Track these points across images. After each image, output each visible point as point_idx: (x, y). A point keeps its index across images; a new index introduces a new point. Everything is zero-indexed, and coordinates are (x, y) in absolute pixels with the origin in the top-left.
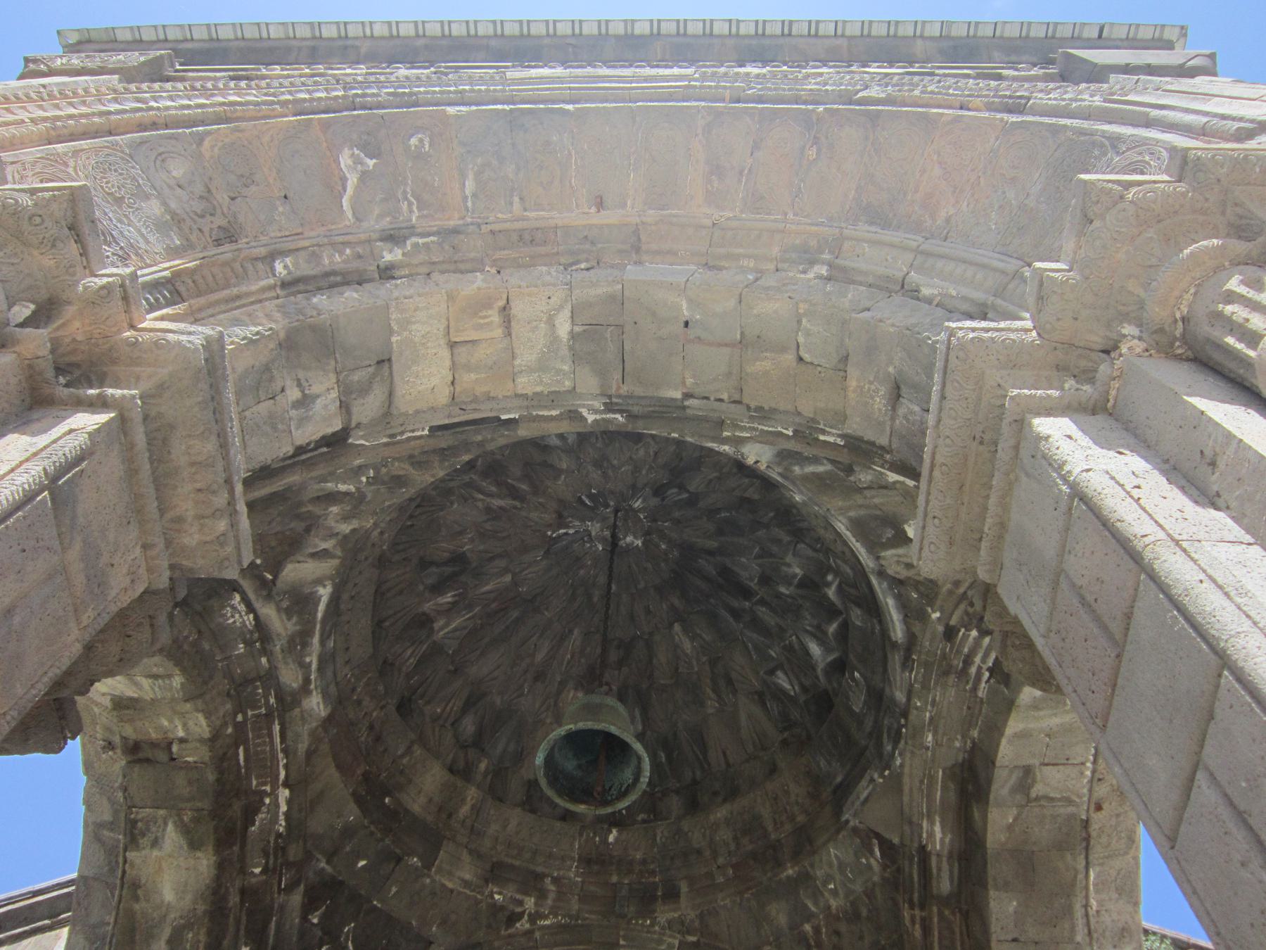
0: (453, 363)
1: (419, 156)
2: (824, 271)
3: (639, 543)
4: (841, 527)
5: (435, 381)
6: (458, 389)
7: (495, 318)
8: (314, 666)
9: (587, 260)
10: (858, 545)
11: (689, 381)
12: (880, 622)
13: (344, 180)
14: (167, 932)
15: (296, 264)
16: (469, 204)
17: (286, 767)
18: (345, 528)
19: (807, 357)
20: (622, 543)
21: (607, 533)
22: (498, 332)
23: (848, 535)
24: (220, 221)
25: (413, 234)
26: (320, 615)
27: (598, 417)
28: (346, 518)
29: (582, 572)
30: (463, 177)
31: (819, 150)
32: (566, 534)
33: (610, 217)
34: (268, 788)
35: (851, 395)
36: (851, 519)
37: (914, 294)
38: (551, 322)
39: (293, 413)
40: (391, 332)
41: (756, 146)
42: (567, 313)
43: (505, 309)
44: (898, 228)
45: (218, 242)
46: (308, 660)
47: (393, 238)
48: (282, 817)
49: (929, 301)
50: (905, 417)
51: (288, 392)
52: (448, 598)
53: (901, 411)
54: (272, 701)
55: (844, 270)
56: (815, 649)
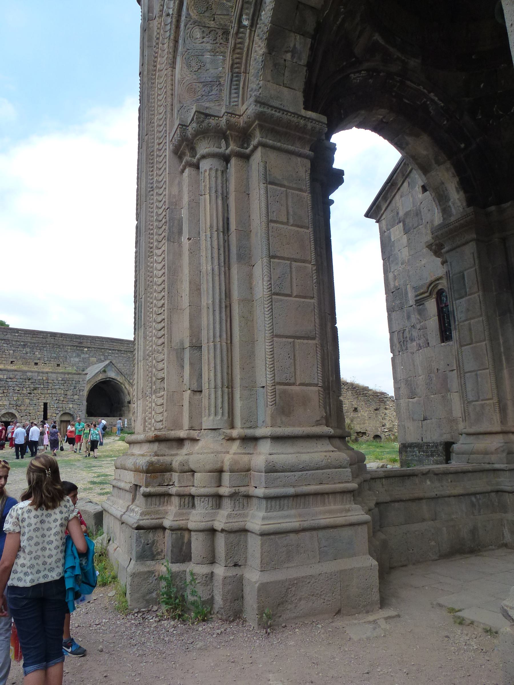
8: (400, 55)
14: (433, 162)
15: (247, 14)
17: (424, 88)
24: (220, 32)
26: (383, 43)
34: (425, 100)
39: (295, 60)
45: (227, 40)
46: (395, 56)
48: (438, 101)
54: (398, 79)
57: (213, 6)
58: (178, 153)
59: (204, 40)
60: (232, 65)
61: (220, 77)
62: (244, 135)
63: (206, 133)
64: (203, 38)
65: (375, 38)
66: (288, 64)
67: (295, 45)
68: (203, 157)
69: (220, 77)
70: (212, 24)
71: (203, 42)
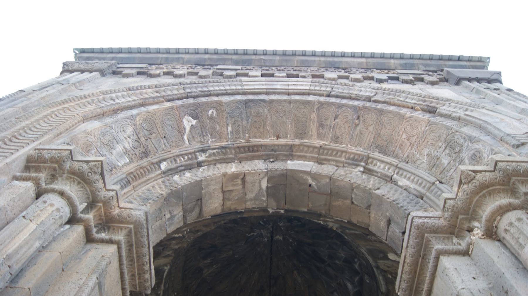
0: (223, 197)
1: (211, 118)
2: (362, 169)
3: (281, 238)
4: (363, 251)
5: (216, 205)
6: (225, 207)
7: (239, 182)
9: (273, 158)
10: (369, 257)
11: (310, 205)
12: (376, 283)
13: (185, 129)
16: (230, 136)
18: (177, 247)
19: (355, 203)
20: (275, 238)
21: (269, 235)
22: (240, 187)
23: (365, 253)
24: (142, 149)
25: (210, 149)
26: (165, 276)
27: (274, 211)
28: (177, 244)
29: (259, 249)
30: (228, 125)
31: (359, 122)
32: (253, 235)
33: (282, 141)
35: (372, 219)
36: (367, 249)
37: (396, 183)
38: (260, 183)
39: (167, 223)
40: (202, 189)
41: (336, 118)
42: (266, 179)
43: (243, 180)
44: (389, 156)
45: (142, 158)
46: (159, 292)
47: (203, 151)
49: (401, 187)
50: (392, 232)
51: (166, 216)
52: (208, 261)
53: (391, 229)
55: (370, 170)
56: (349, 286)
57: (154, 135)
58: (32, 164)
59: (128, 139)
60: (132, 173)
61: (115, 168)
62: (107, 223)
63: (86, 183)
64: (129, 137)
65: (166, 268)
66: (164, 219)
67: (176, 215)
68: (62, 194)
69: (115, 168)
70: (143, 139)
71: (126, 138)
